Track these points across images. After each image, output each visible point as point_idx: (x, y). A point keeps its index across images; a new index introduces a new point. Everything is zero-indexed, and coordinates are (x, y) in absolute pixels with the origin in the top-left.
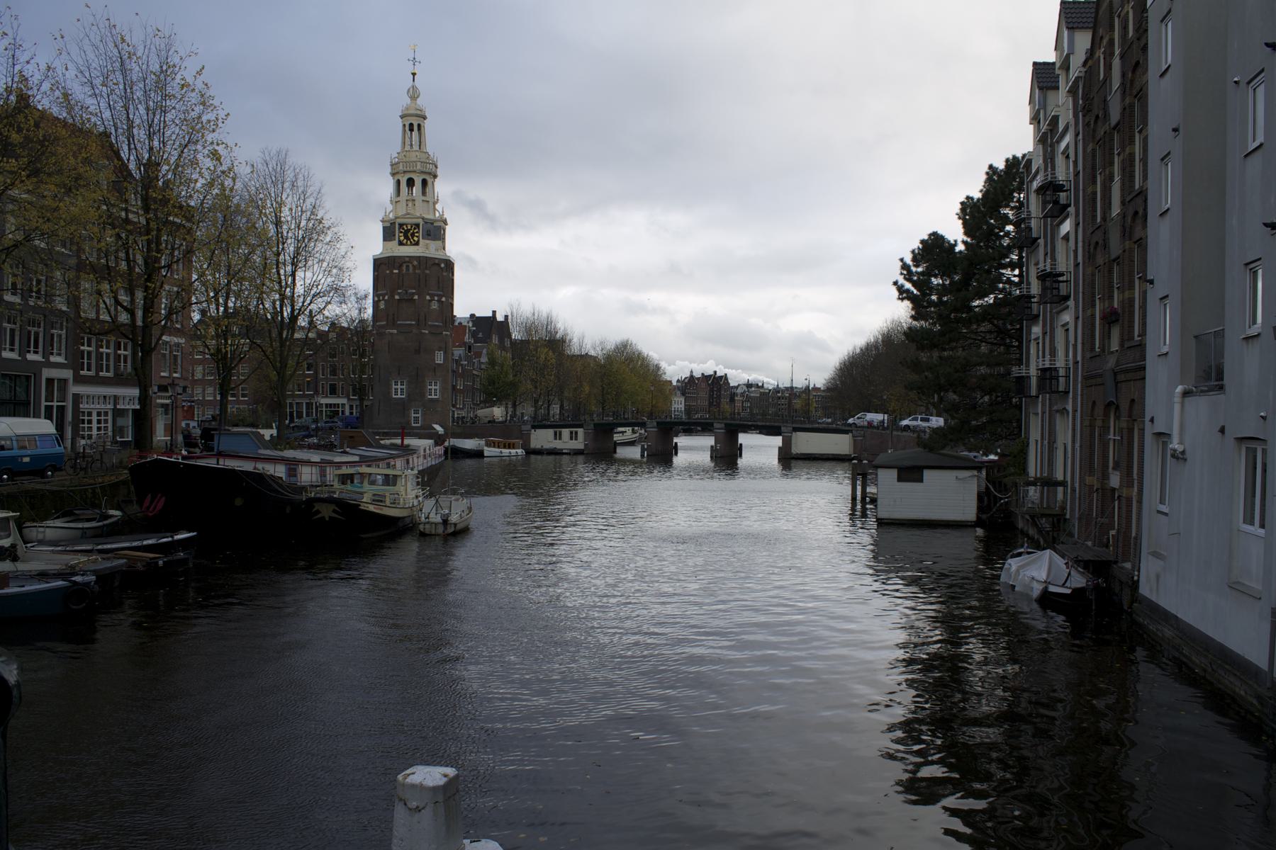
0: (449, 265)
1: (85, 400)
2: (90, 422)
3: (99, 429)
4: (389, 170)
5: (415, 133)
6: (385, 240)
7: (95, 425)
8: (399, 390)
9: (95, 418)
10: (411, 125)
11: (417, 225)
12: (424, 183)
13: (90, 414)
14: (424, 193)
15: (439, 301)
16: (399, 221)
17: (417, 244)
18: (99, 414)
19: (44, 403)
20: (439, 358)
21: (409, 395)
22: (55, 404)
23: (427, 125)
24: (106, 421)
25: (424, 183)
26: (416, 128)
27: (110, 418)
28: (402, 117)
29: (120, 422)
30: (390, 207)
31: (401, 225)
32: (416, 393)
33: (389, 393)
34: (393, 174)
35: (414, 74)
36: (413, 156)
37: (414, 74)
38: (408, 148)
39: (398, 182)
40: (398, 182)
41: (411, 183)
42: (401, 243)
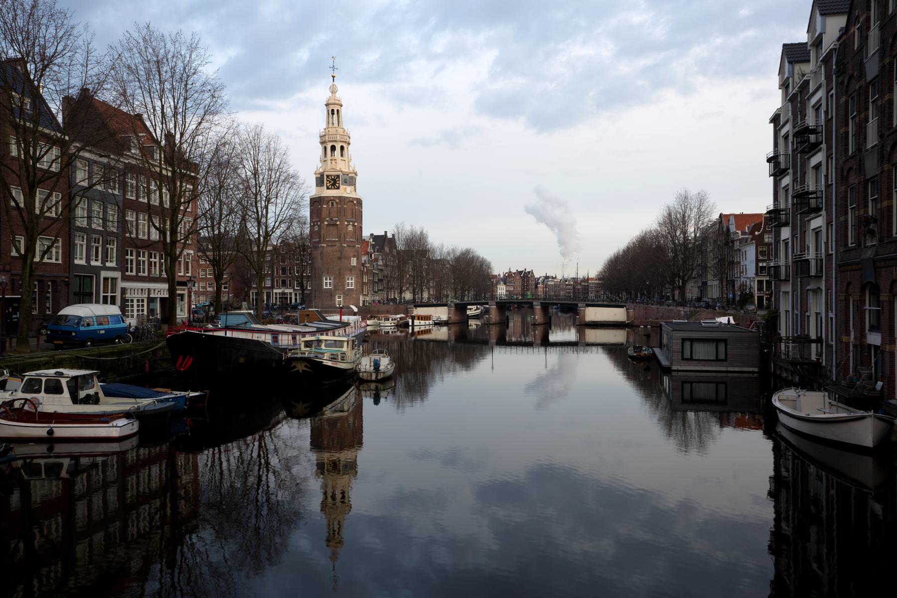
0: (359, 202)
1: (129, 291)
2: (132, 306)
3: (138, 311)
4: (319, 140)
5: (335, 116)
6: (317, 185)
7: (135, 308)
8: (327, 283)
9: (135, 303)
10: (333, 110)
11: (338, 176)
12: (342, 148)
13: (132, 301)
14: (342, 155)
15: (353, 225)
16: (326, 173)
17: (338, 188)
18: (138, 301)
19: (102, 294)
20: (354, 262)
21: (334, 287)
22: (109, 294)
23: (343, 111)
24: (143, 306)
25: (342, 148)
26: (336, 112)
27: (145, 303)
28: (327, 105)
29: (152, 306)
30: (320, 165)
31: (328, 176)
32: (339, 284)
33: (322, 285)
34: (322, 143)
35: (333, 77)
36: (332, 131)
37: (333, 77)
38: (331, 125)
39: (325, 148)
40: (325, 148)
41: (333, 148)
42: (328, 188)
